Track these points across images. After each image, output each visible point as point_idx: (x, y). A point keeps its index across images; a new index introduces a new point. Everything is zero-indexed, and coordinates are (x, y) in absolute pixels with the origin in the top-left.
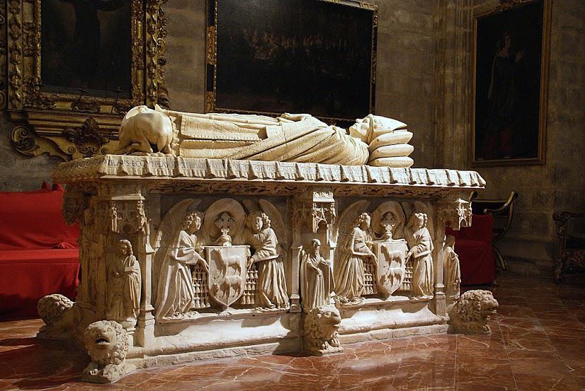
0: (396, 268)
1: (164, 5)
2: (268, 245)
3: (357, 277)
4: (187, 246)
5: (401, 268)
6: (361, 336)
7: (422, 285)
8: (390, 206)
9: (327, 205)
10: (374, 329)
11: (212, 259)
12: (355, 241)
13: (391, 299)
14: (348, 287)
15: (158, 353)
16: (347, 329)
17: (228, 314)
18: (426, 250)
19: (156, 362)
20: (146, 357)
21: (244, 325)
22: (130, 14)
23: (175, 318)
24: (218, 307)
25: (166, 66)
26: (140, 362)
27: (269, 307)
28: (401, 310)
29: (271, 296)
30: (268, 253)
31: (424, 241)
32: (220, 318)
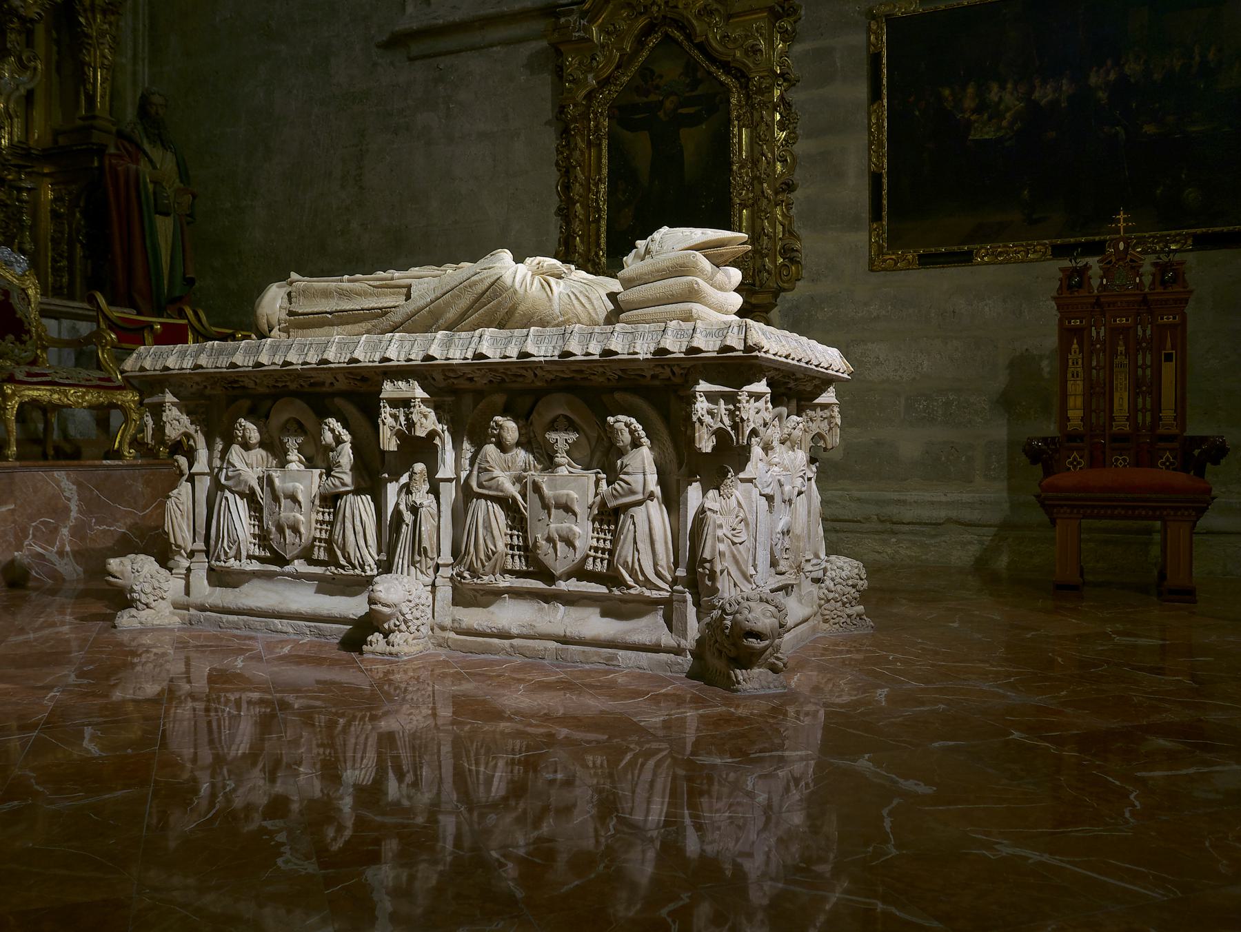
0: (557, 524)
1: (793, 89)
2: (337, 470)
3: (481, 530)
4: (234, 466)
5: (584, 533)
6: (490, 644)
7: (625, 565)
8: (558, 407)
9: (406, 403)
10: (519, 636)
11: (267, 486)
12: (479, 468)
13: (572, 585)
14: (467, 552)
15: (202, 608)
16: (464, 625)
17: (294, 571)
18: (633, 492)
19: (202, 620)
20: (192, 611)
21: (319, 591)
22: (729, 122)
23: (223, 564)
24: (280, 560)
25: (798, 195)
26: (184, 615)
27: (343, 567)
28: (598, 610)
29: (344, 549)
30: (337, 483)
31: (626, 473)
32: (289, 575)
